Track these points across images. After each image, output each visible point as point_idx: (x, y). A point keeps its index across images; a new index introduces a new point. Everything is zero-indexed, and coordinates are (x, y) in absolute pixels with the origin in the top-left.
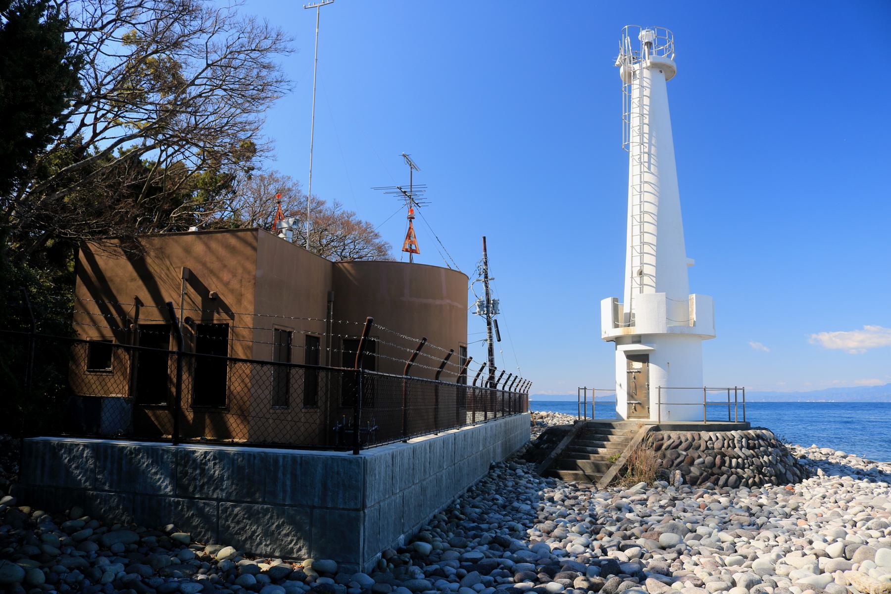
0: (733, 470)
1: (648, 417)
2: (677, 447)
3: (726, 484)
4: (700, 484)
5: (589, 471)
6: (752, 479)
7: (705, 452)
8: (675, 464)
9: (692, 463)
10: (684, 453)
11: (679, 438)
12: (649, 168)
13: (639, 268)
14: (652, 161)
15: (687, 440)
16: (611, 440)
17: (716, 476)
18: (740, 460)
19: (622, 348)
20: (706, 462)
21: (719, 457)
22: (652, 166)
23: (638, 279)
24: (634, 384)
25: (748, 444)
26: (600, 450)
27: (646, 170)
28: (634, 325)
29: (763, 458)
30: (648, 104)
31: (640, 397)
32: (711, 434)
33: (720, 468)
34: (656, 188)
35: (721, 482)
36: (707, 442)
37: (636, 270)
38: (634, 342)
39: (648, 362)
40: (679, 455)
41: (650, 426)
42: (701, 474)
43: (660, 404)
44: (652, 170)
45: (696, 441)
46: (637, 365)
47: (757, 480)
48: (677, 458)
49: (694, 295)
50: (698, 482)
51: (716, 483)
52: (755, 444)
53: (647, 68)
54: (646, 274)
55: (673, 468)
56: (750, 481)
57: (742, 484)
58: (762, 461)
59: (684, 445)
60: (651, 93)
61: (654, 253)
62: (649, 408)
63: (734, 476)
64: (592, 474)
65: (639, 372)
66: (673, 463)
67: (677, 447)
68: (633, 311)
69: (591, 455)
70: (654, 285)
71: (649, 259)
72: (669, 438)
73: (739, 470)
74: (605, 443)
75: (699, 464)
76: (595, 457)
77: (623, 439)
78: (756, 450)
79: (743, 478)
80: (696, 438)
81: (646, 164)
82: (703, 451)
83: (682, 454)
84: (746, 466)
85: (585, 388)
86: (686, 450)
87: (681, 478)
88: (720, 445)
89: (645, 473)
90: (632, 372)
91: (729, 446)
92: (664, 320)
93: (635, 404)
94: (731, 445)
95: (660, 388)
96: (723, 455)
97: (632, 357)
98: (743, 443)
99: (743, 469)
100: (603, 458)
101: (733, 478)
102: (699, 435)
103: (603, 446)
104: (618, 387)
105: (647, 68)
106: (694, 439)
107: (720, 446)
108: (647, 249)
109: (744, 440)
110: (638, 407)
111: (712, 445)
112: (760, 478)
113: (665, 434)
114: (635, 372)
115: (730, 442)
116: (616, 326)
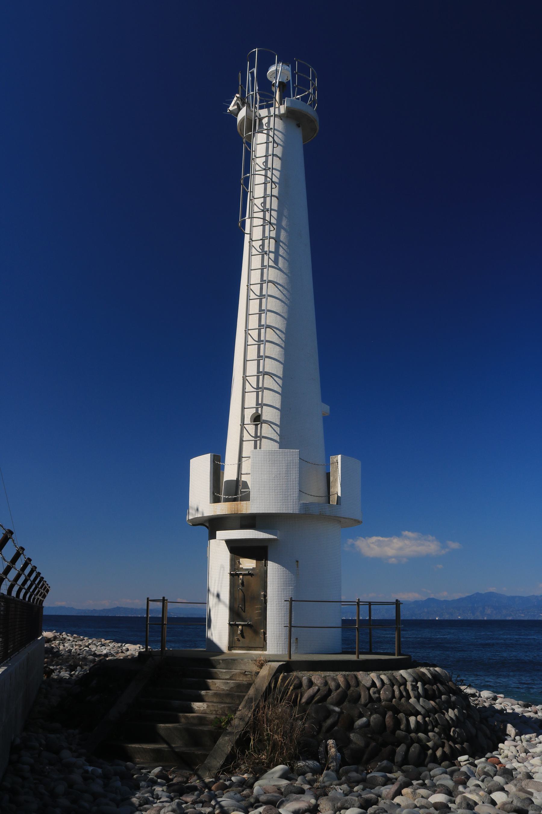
0: (413, 735)
1: (264, 648)
2: (324, 698)
3: (405, 761)
4: (368, 762)
5: (178, 745)
6: (440, 749)
7: (369, 705)
8: (324, 729)
9: (350, 727)
10: (337, 709)
11: (326, 684)
12: (276, 261)
13: (254, 411)
14: (281, 251)
15: (338, 686)
16: (212, 688)
17: (389, 747)
18: (419, 718)
19: (222, 535)
20: (372, 724)
21: (389, 714)
22: (280, 258)
23: (251, 428)
24: (241, 593)
25: (425, 690)
26: (197, 705)
27: (271, 263)
28: (246, 498)
29: (448, 712)
30: (279, 169)
31: (253, 614)
32: (373, 675)
33: (393, 732)
34: (285, 292)
35: (398, 758)
36: (369, 689)
37: (249, 414)
38: (243, 527)
39: (266, 560)
40: (329, 713)
41: (276, 665)
42: (367, 745)
43: (291, 627)
44: (280, 265)
45: (352, 689)
46: (248, 564)
47: (447, 749)
48: (327, 717)
49: (339, 457)
50: (365, 758)
51: (391, 757)
52: (434, 690)
53: (281, 117)
54: (266, 422)
55: (321, 736)
56: (439, 753)
57: (427, 760)
58: (448, 719)
59: (334, 695)
60: (284, 153)
61: (279, 389)
62: (265, 633)
63: (415, 745)
64: (184, 749)
65: (249, 574)
66: (321, 727)
67: (324, 698)
68: (244, 478)
69: (181, 714)
70: (277, 438)
71: (270, 398)
72: (311, 683)
73: (421, 735)
74: (203, 692)
75: (362, 727)
76: (187, 718)
77: (232, 685)
78: (437, 700)
79: (428, 748)
80: (353, 683)
81: (272, 256)
82: (365, 705)
83: (334, 711)
84: (430, 727)
85: (164, 600)
86: (338, 703)
87: (338, 754)
88: (389, 694)
89: (282, 748)
90: (238, 575)
91: (401, 696)
92: (295, 494)
93: (243, 625)
94: (404, 694)
95: (291, 601)
96: (396, 711)
97: (233, 545)
98: (420, 690)
99: (426, 732)
100: (202, 720)
101: (415, 748)
102: (356, 678)
103: (201, 699)
104: (212, 600)
105: (281, 117)
106: (348, 686)
107: (390, 696)
108: (268, 382)
109: (419, 684)
110: (248, 633)
111: (377, 695)
112: (450, 746)
113: (304, 676)
114: (244, 575)
115: (402, 688)
116: (216, 499)
